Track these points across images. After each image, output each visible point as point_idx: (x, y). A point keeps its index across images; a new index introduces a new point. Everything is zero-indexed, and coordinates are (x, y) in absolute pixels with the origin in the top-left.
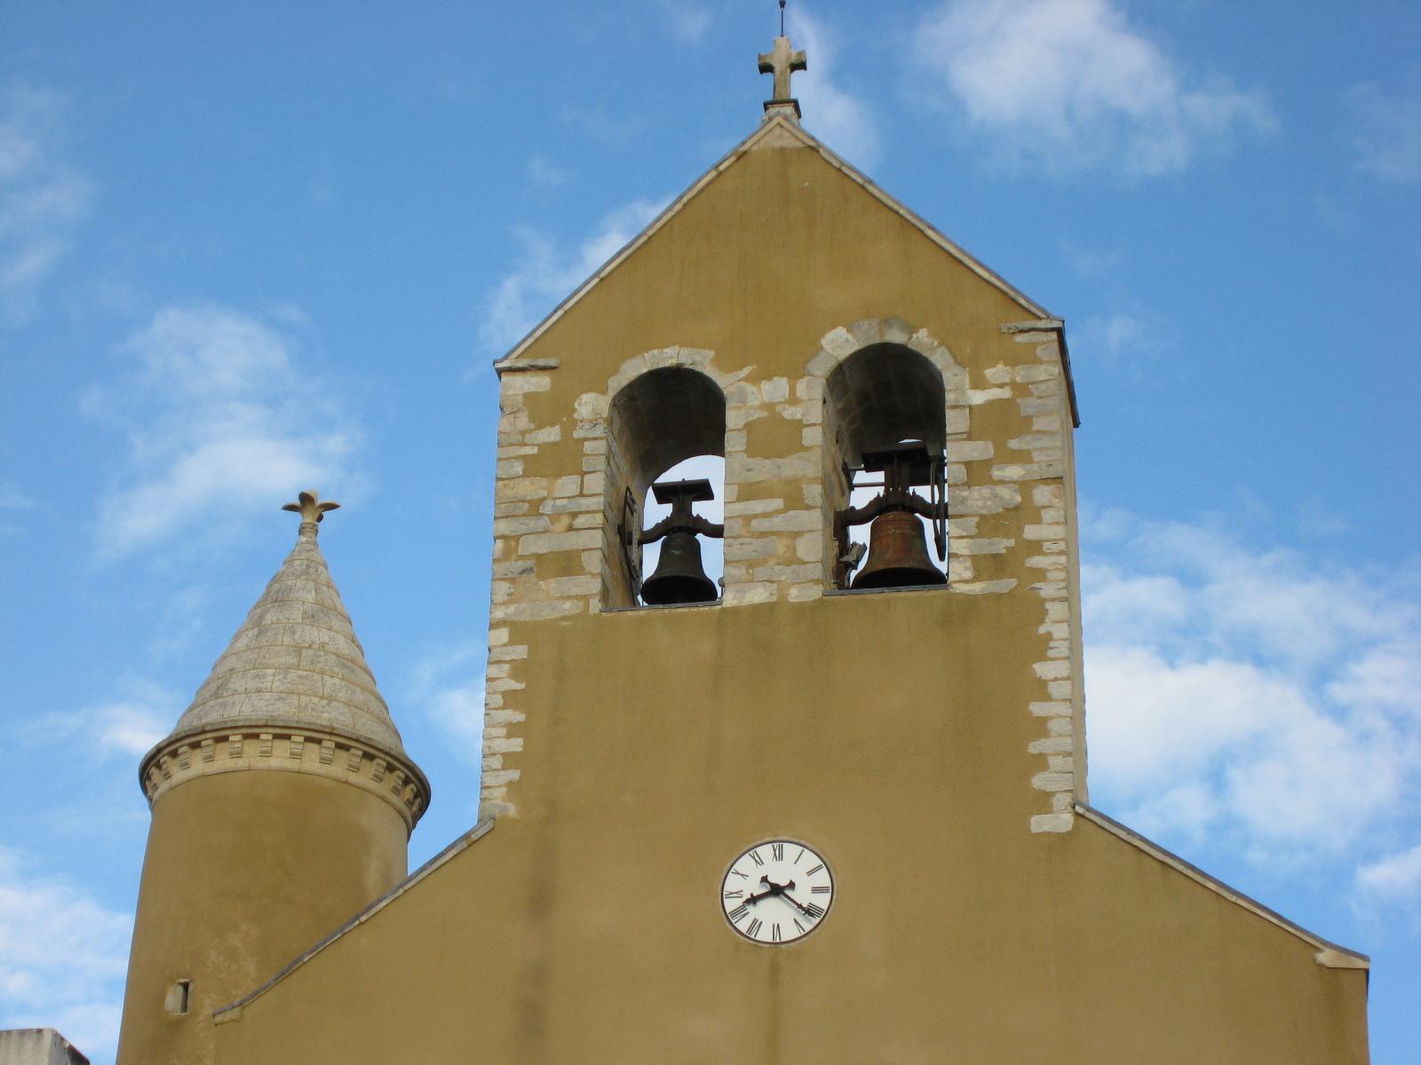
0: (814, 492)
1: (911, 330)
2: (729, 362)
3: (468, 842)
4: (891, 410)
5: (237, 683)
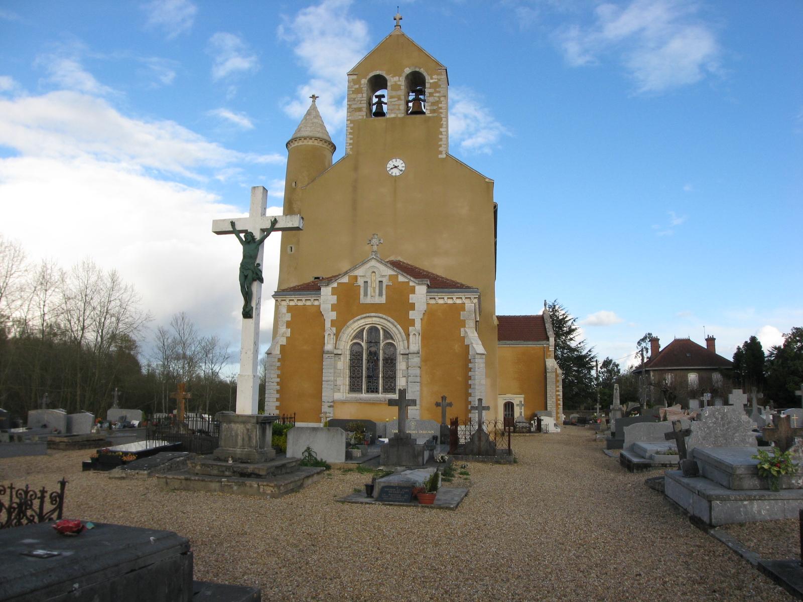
0: (403, 97)
1: (420, 68)
2: (389, 73)
3: (343, 158)
4: (416, 82)
5: (302, 129)
